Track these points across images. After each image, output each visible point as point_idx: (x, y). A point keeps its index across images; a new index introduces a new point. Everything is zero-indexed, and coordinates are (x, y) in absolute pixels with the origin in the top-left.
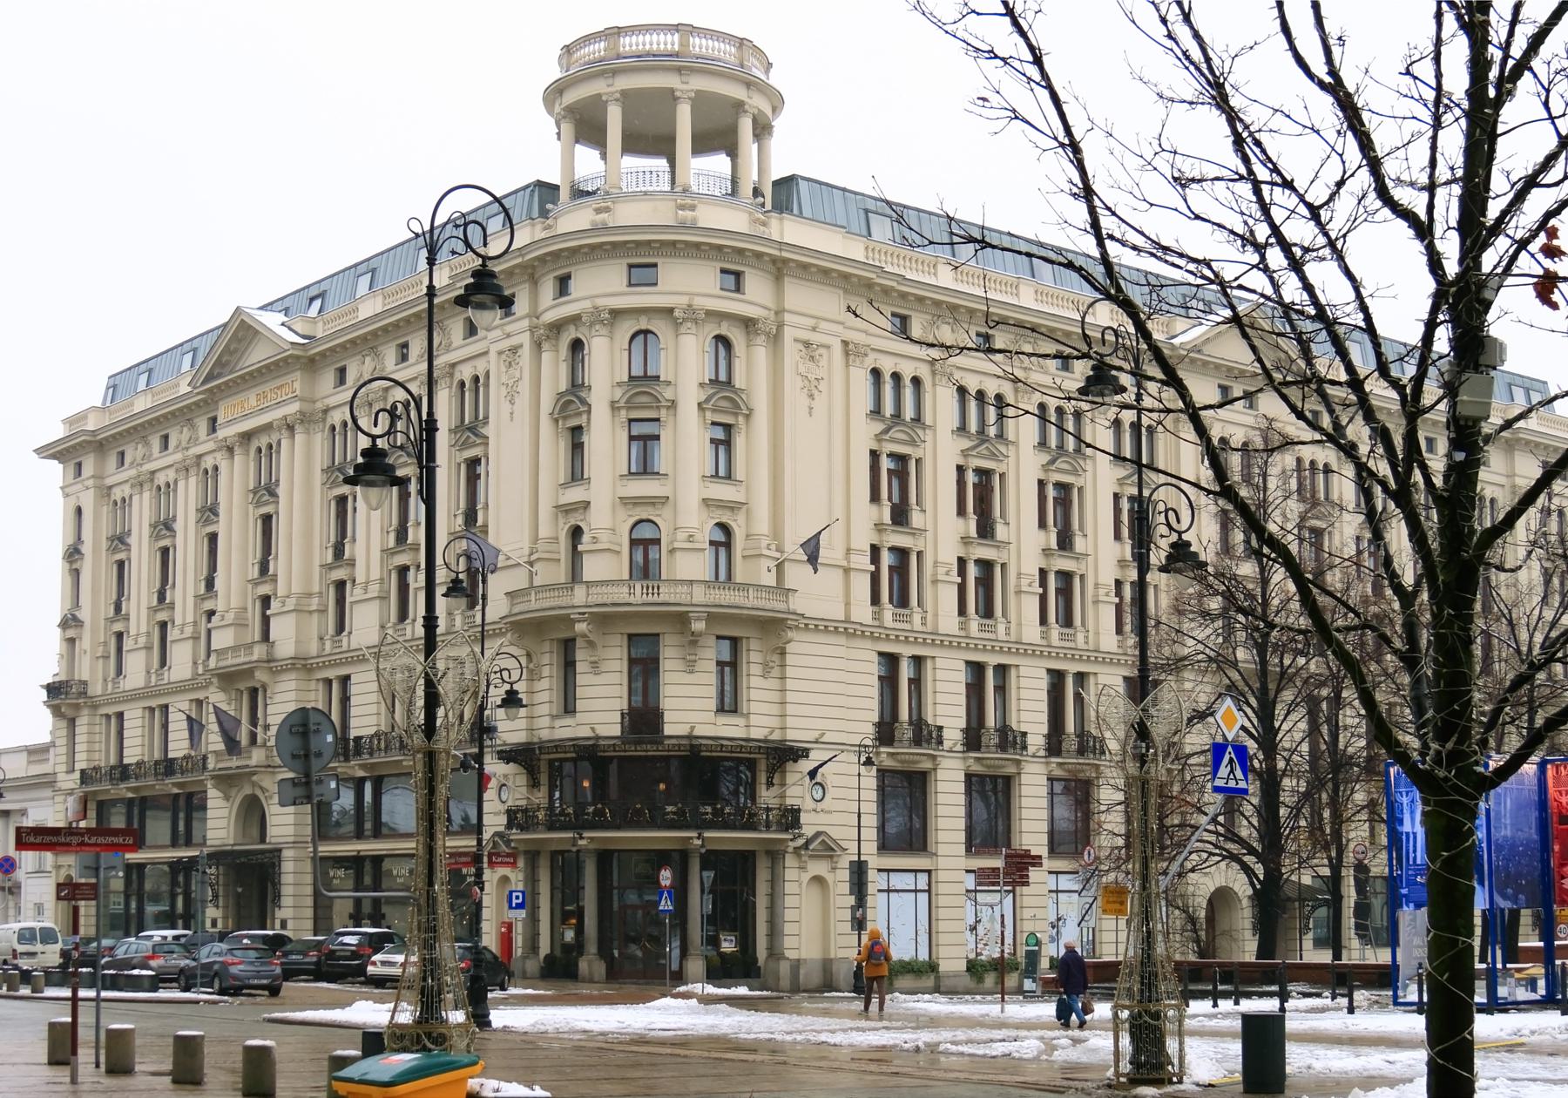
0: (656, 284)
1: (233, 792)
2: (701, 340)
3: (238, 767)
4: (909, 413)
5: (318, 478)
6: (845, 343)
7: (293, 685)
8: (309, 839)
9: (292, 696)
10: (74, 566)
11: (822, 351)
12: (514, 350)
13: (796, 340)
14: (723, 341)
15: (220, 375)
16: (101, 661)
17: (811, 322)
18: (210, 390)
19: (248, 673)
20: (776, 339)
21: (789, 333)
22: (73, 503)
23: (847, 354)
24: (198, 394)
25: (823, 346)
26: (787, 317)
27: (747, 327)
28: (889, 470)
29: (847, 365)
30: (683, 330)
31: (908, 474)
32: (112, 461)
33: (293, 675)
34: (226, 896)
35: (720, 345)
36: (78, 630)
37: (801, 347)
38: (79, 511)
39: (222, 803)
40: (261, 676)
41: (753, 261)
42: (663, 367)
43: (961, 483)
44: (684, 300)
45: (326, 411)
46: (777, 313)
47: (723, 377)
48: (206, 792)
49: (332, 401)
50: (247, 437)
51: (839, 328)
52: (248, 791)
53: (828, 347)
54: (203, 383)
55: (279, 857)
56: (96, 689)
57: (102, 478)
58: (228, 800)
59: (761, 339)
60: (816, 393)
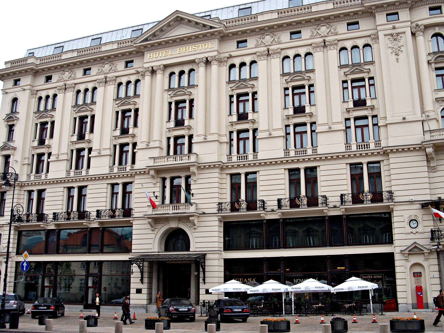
1: (159, 226)
3: (173, 213)
5: (224, 84)
7: (217, 175)
8: (222, 249)
9: (217, 180)
10: (11, 123)
12: (398, 34)
15: (151, 40)
16: (26, 166)
18: (145, 47)
19: (187, 168)
22: (10, 97)
24: (135, 47)
32: (42, 79)
33: (217, 170)
34: (150, 278)
36: (13, 151)
38: (15, 100)
39: (149, 231)
40: (193, 169)
45: (231, 57)
48: (132, 226)
49: (233, 54)
50: (166, 67)
52: (174, 225)
54: (140, 42)
55: (205, 258)
56: (23, 178)
57: (33, 87)
58: (153, 230)
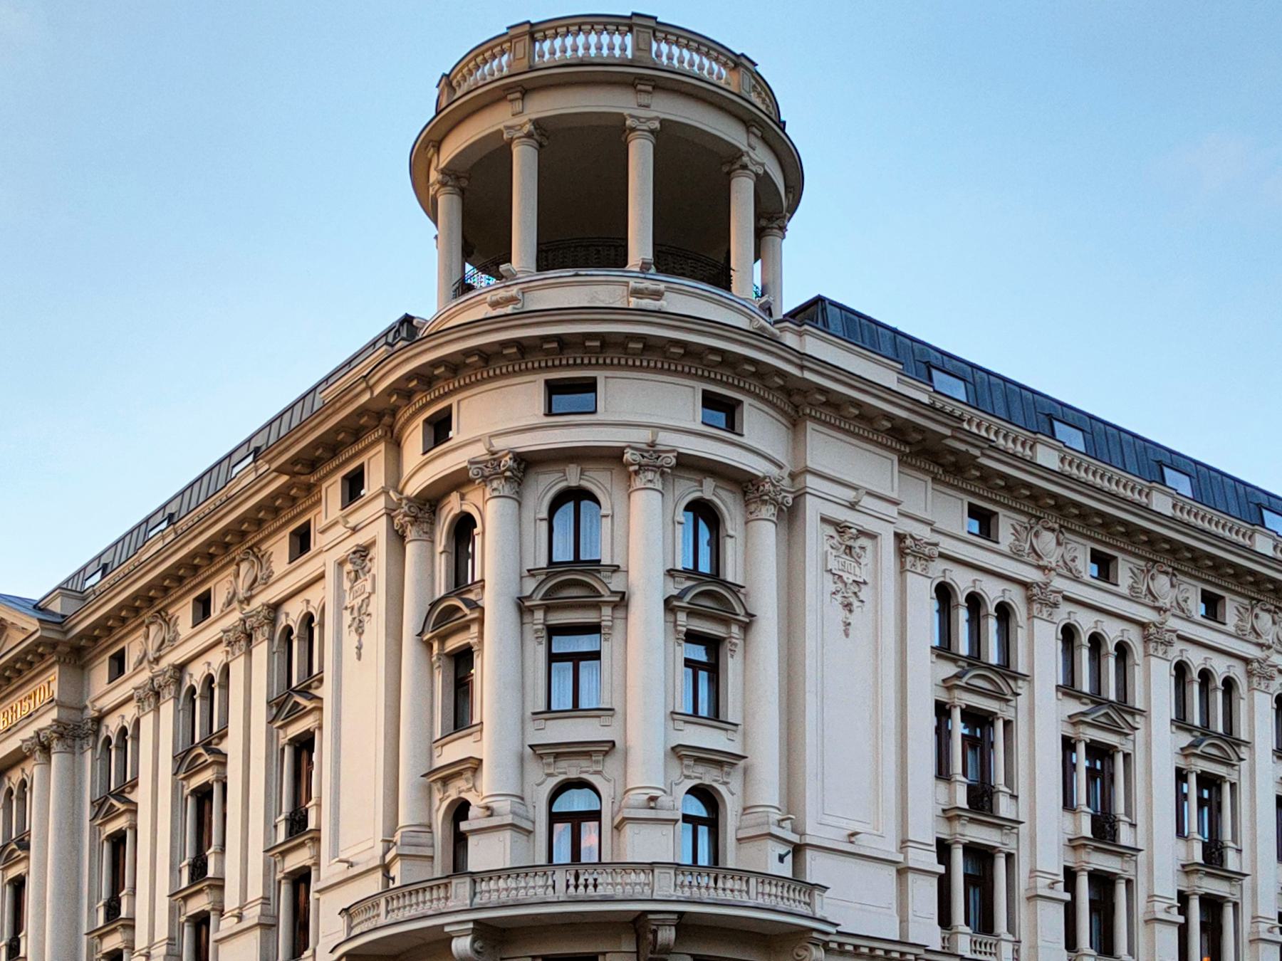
0: (595, 412)
2: (671, 505)
4: (993, 655)
6: (900, 538)
11: (863, 541)
13: (824, 520)
14: (703, 511)
17: (850, 495)
20: (790, 515)
21: (813, 509)
23: (901, 553)
25: (862, 533)
26: (811, 481)
27: (745, 493)
28: (963, 735)
29: (903, 571)
30: (638, 482)
31: (992, 745)
35: (702, 525)
37: (831, 530)
41: (754, 386)
42: (602, 548)
43: (1068, 769)
44: (642, 437)
46: (793, 476)
47: (705, 567)
51: (892, 511)
53: (872, 536)
59: (768, 511)
60: (856, 604)
